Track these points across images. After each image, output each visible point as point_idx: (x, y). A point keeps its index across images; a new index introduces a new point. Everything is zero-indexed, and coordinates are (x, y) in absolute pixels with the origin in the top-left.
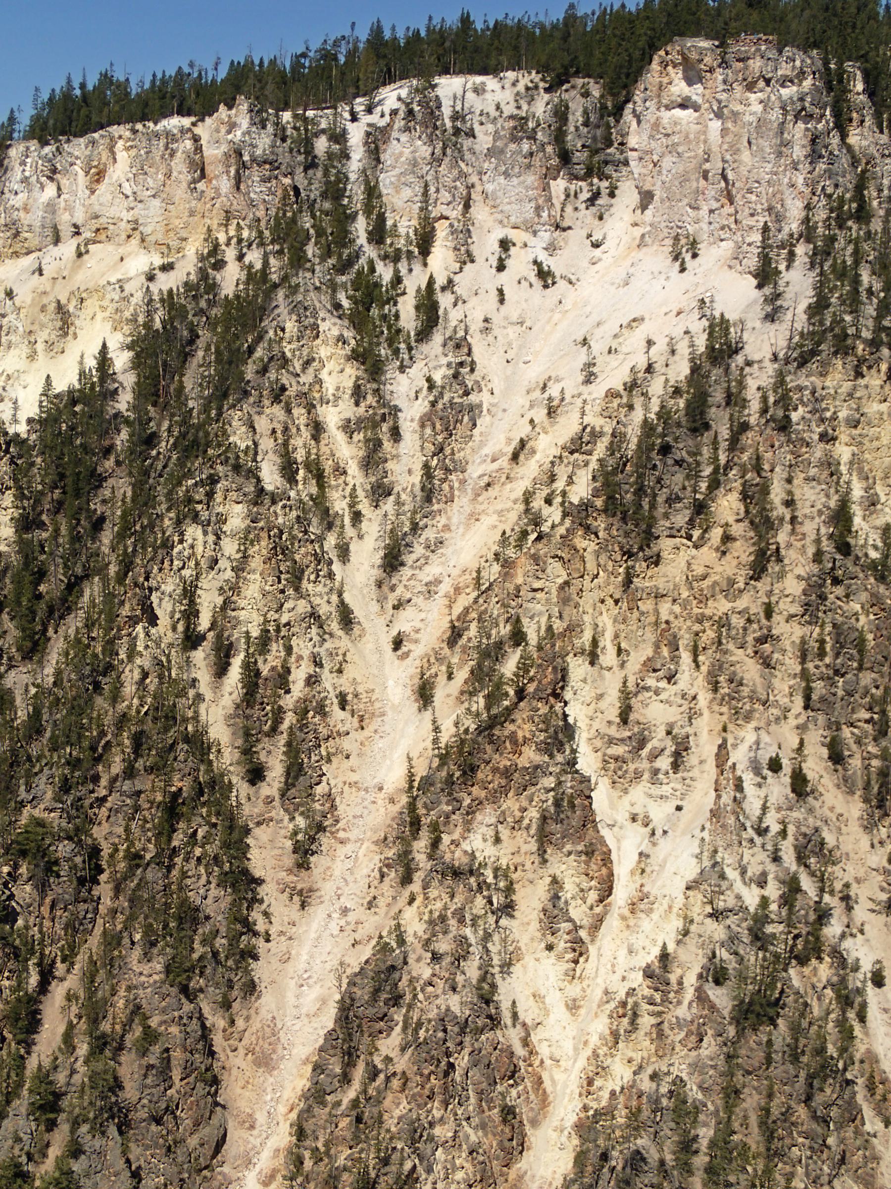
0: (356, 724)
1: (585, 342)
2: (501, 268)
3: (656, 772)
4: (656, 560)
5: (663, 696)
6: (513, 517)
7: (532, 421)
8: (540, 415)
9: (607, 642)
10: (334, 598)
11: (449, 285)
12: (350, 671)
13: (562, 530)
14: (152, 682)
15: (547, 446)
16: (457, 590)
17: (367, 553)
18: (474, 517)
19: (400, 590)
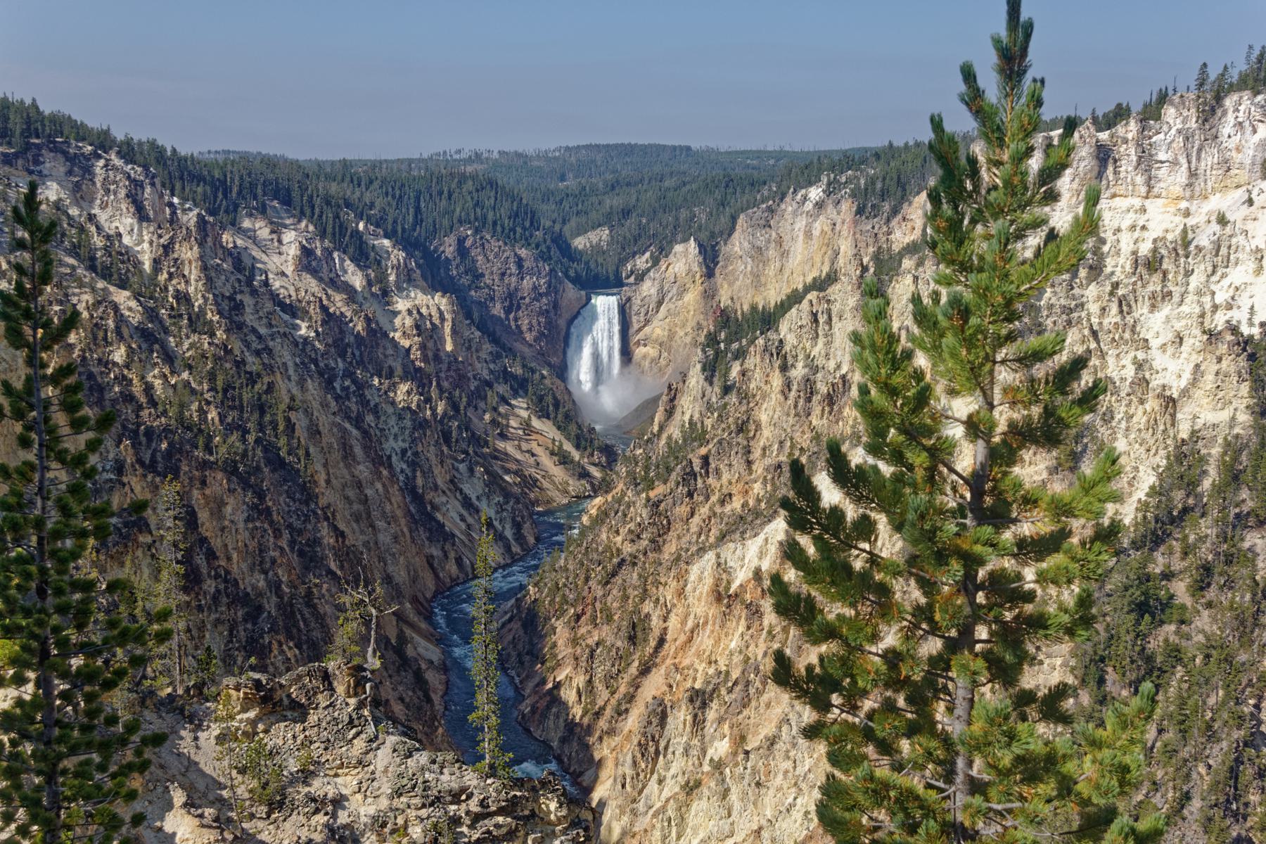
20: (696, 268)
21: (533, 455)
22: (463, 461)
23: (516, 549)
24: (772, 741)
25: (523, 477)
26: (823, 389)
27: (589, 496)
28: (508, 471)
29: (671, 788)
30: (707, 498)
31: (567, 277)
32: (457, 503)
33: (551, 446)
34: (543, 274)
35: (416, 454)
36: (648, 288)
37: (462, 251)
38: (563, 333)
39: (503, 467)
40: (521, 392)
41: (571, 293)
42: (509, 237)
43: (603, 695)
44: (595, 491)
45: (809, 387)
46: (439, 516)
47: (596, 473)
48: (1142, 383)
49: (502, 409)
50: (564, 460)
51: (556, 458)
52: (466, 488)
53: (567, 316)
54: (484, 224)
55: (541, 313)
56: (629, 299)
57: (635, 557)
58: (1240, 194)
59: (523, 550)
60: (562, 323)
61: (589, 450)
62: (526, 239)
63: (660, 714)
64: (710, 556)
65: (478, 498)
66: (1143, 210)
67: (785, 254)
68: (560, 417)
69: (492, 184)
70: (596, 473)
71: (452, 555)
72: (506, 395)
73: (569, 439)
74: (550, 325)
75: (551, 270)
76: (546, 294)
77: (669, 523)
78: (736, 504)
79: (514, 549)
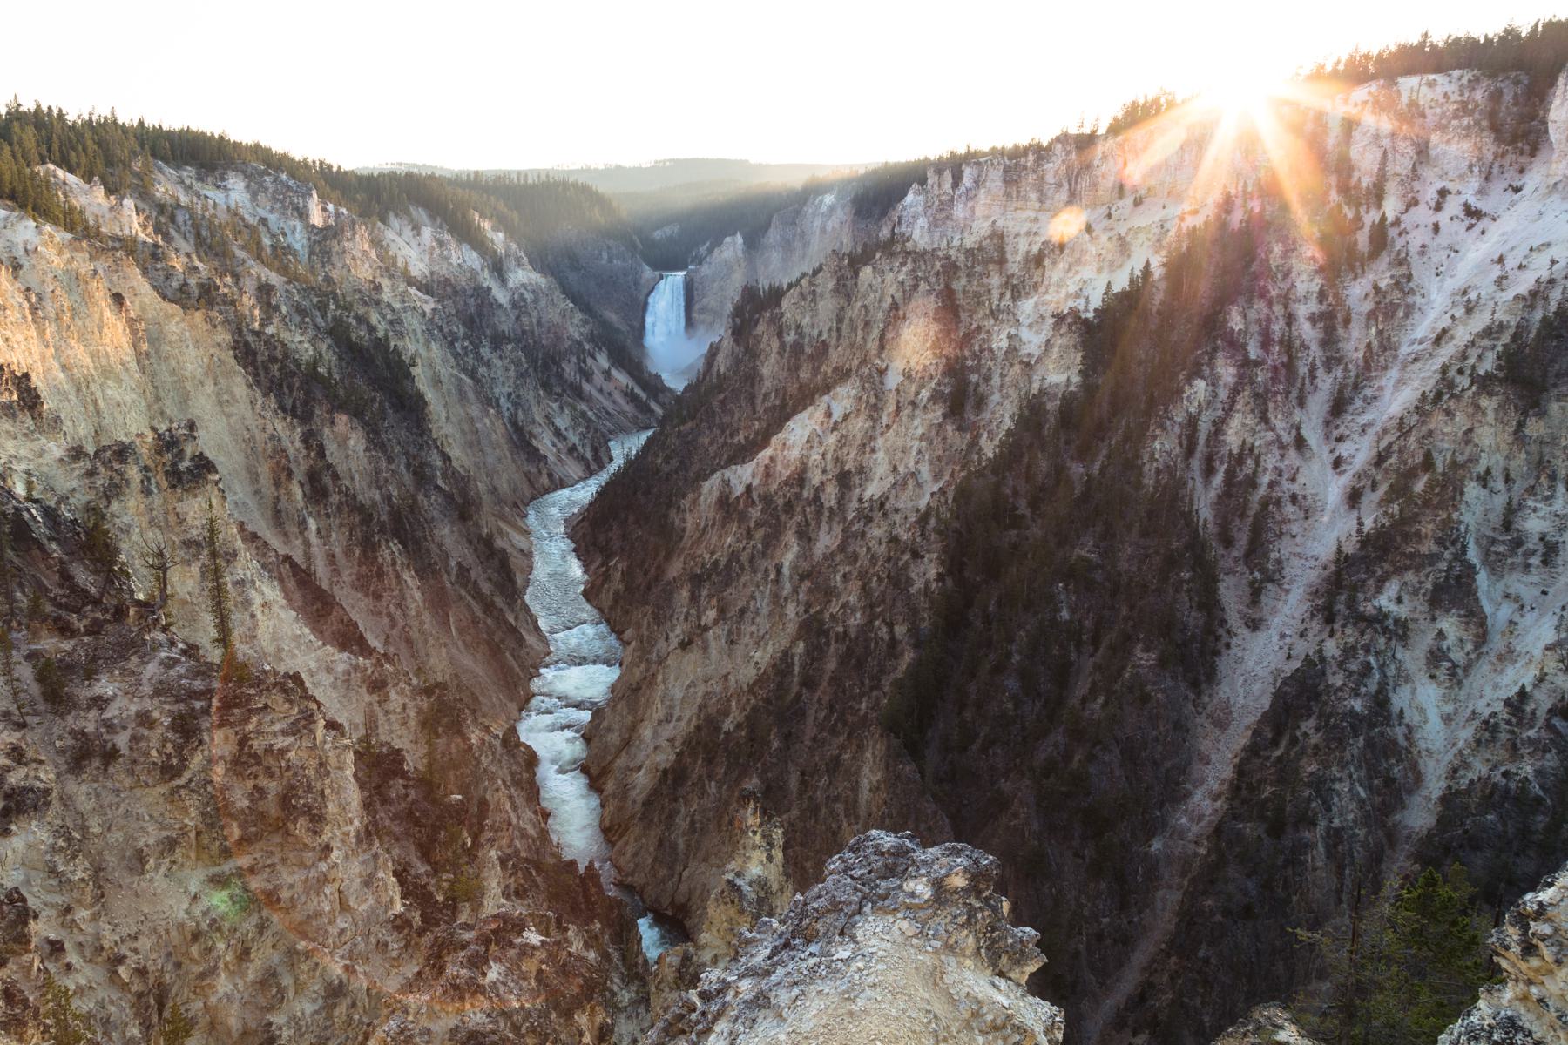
0: (1302, 515)
1: (1501, 260)
2: (1438, 208)
3: (1528, 566)
4: (1543, 414)
5: (1541, 514)
6: (1432, 382)
7: (1453, 317)
8: (1459, 312)
9: (1497, 473)
10: (1294, 432)
11: (1397, 222)
12: (1301, 479)
13: (1470, 393)
14: (1164, 479)
15: (1462, 335)
16: (1385, 431)
17: (1318, 404)
18: (1401, 382)
19: (1342, 429)
20: (740, 254)
23: (594, 466)
24: (743, 611)
26: (808, 350)
29: (674, 642)
30: (723, 432)
35: (518, 397)
36: (705, 270)
43: (640, 580)
45: (798, 348)
46: (535, 443)
48: (1012, 351)
50: (631, 397)
53: (645, 291)
58: (1103, 210)
63: (669, 594)
64: (718, 475)
66: (1036, 220)
67: (806, 245)
71: (545, 472)
78: (741, 437)
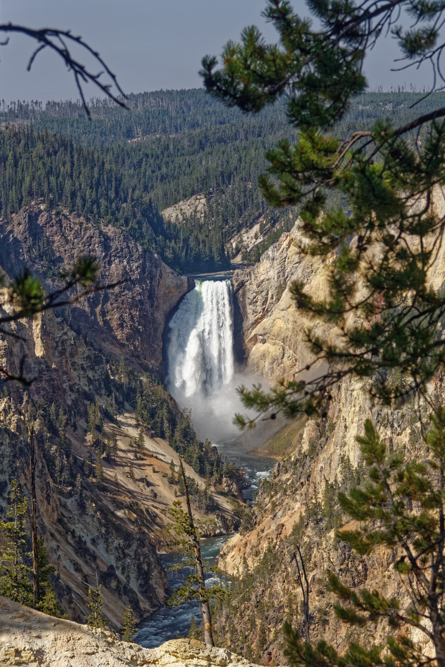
21: (149, 484)
22: (70, 495)
23: (144, 605)
25: (139, 512)
27: (221, 534)
28: (120, 506)
31: (165, 259)
32: (69, 549)
33: (169, 472)
34: (136, 256)
37: (34, 231)
38: (161, 329)
39: (114, 501)
40: (127, 405)
41: (169, 278)
42: (92, 212)
44: (227, 528)
47: (226, 504)
49: (107, 427)
51: (176, 487)
52: (78, 528)
53: (165, 307)
54: (61, 195)
55: (133, 305)
56: (242, 284)
57: (326, 613)
59: (153, 606)
60: (160, 316)
61: (216, 475)
62: (113, 214)
65: (94, 541)
68: (178, 435)
69: (65, 145)
70: (226, 504)
72: (110, 409)
73: (190, 463)
74: (145, 318)
75: (145, 251)
76: (141, 281)
77: (366, 570)
79: (142, 605)
